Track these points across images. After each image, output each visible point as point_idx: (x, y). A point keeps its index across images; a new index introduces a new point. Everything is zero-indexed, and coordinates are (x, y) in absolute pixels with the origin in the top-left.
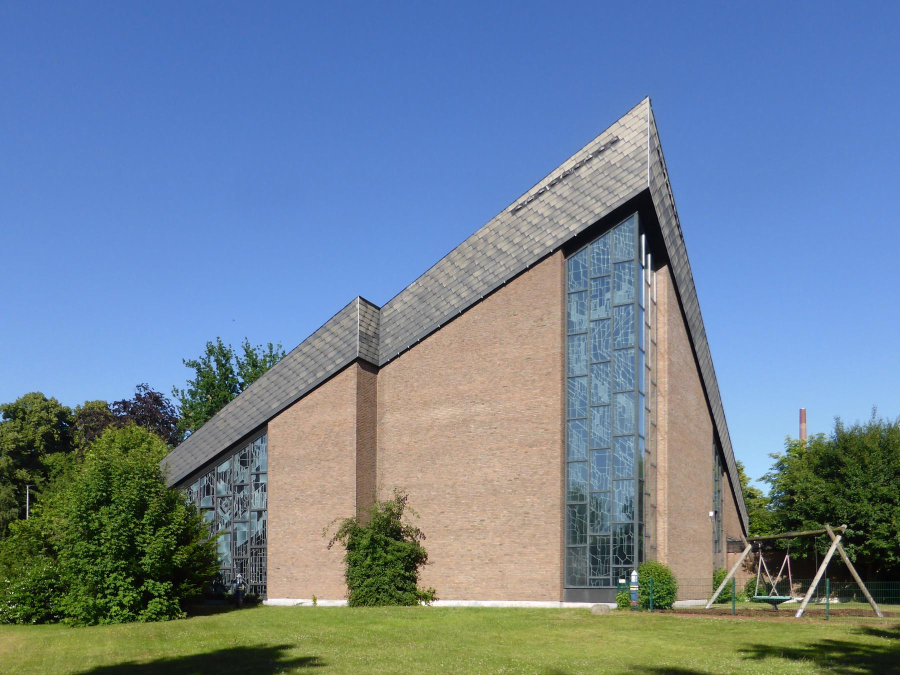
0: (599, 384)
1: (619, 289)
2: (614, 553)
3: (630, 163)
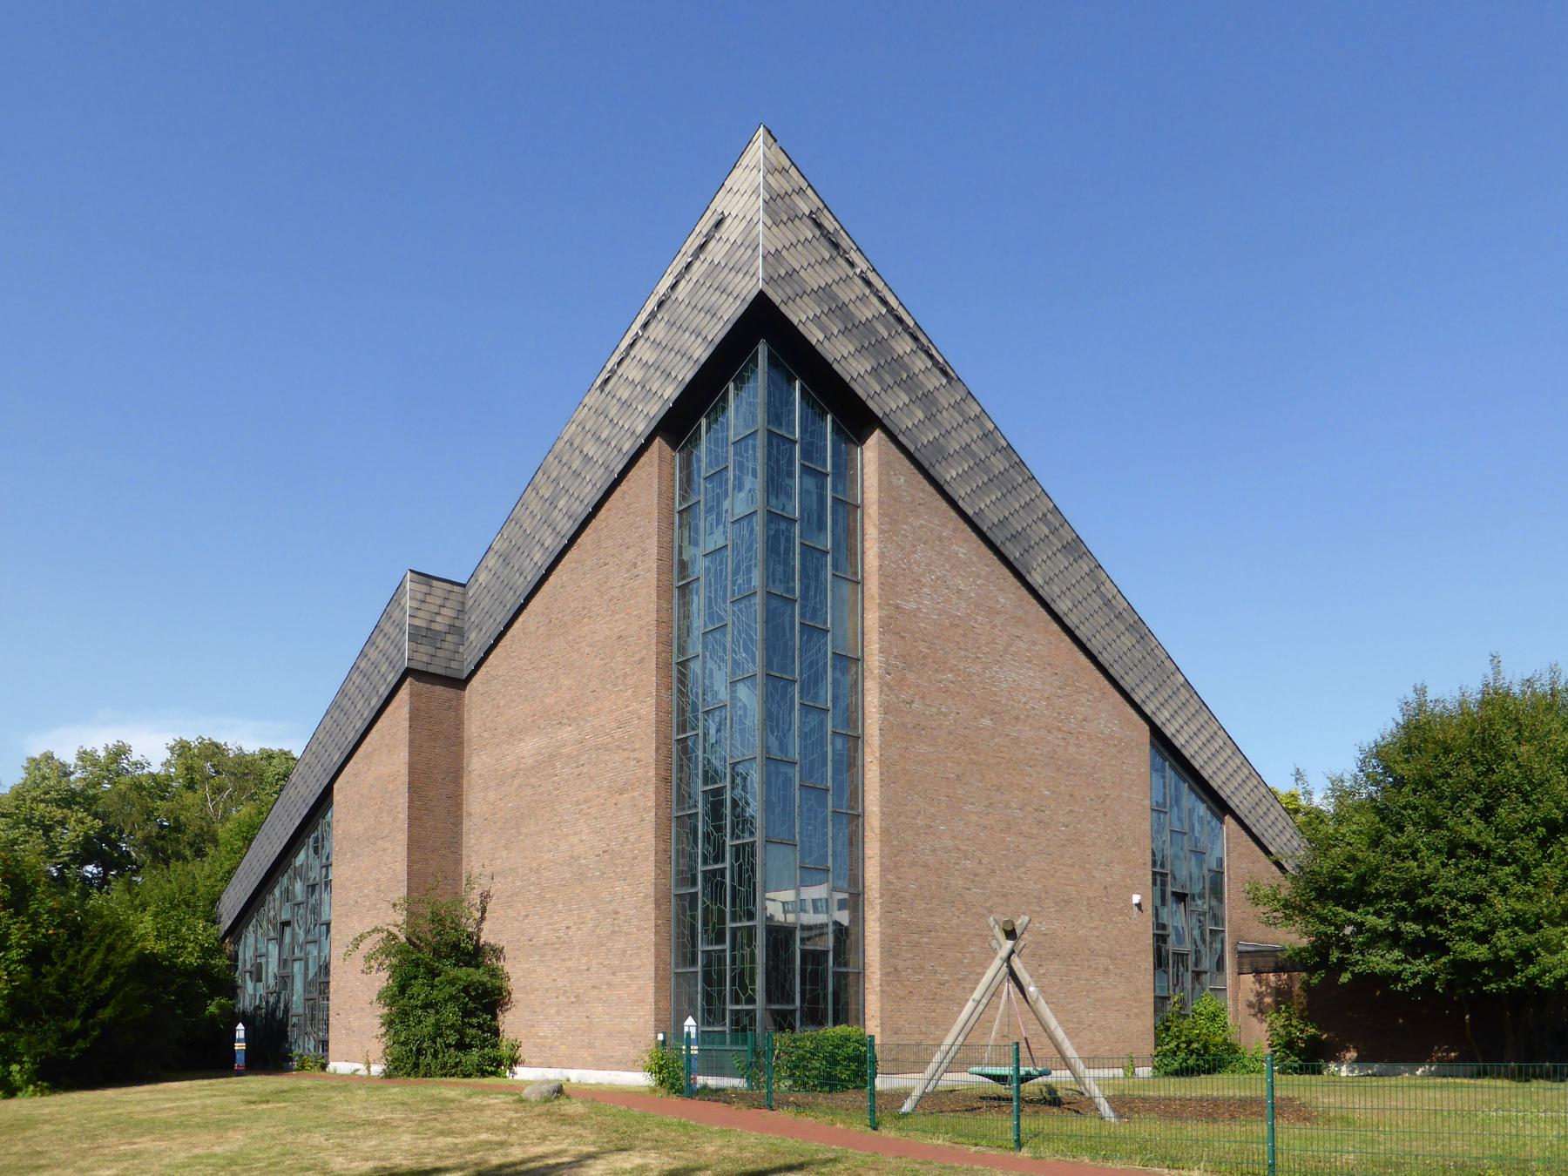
0: (715, 667)
1: (740, 490)
3: (738, 254)
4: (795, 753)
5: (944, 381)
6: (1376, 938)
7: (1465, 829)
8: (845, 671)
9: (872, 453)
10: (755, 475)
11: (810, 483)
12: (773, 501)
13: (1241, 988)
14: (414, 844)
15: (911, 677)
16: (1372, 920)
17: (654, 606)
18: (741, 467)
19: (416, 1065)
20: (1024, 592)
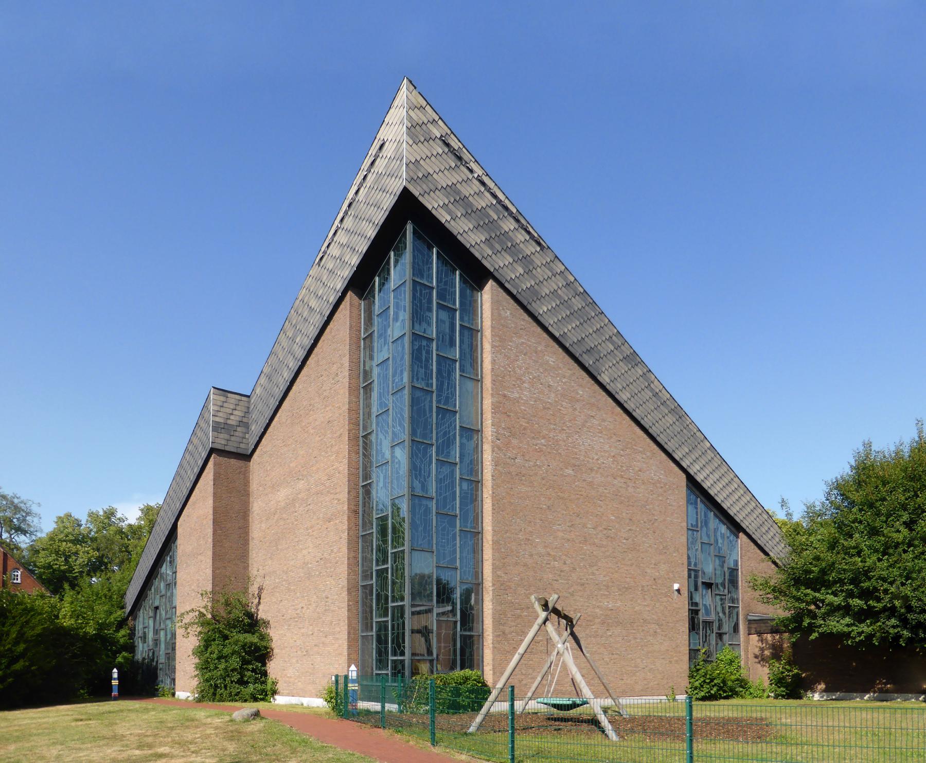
0: (383, 438)
1: (397, 321)
2: (393, 642)
4: (433, 491)
5: (538, 249)
6: (834, 610)
7: (895, 535)
8: (470, 438)
9: (488, 295)
10: (405, 311)
11: (444, 315)
12: (417, 326)
13: (749, 646)
14: (217, 557)
15: (515, 442)
16: (830, 598)
17: (347, 400)
18: (397, 306)
19: (214, 694)
20: (597, 387)
